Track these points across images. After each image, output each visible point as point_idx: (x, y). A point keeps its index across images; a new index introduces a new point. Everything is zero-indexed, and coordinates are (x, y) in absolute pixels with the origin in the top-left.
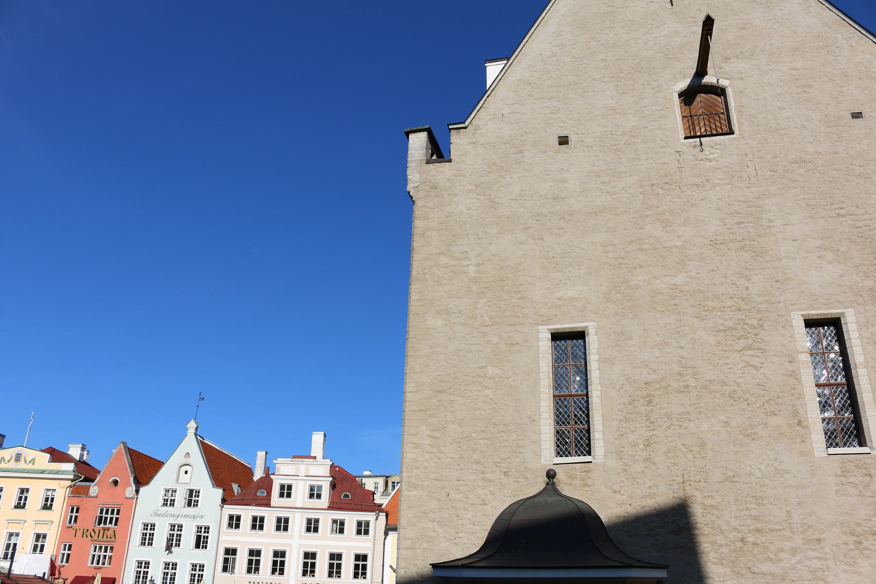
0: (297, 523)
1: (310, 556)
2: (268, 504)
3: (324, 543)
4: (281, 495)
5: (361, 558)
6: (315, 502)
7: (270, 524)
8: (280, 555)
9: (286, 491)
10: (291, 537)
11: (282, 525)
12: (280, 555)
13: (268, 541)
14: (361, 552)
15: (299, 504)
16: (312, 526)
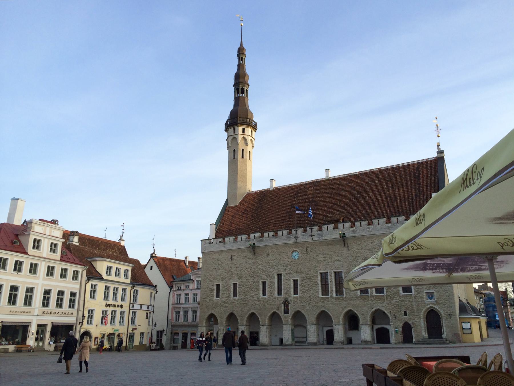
0: (42, 269)
1: (47, 292)
2: (26, 253)
3: (56, 284)
4: (34, 248)
5: (73, 294)
6: (52, 256)
7: (26, 267)
8: (30, 290)
9: (37, 244)
10: (38, 278)
11: (33, 269)
12: (30, 290)
13: (23, 280)
14: (74, 291)
15: (45, 255)
16: (50, 271)
